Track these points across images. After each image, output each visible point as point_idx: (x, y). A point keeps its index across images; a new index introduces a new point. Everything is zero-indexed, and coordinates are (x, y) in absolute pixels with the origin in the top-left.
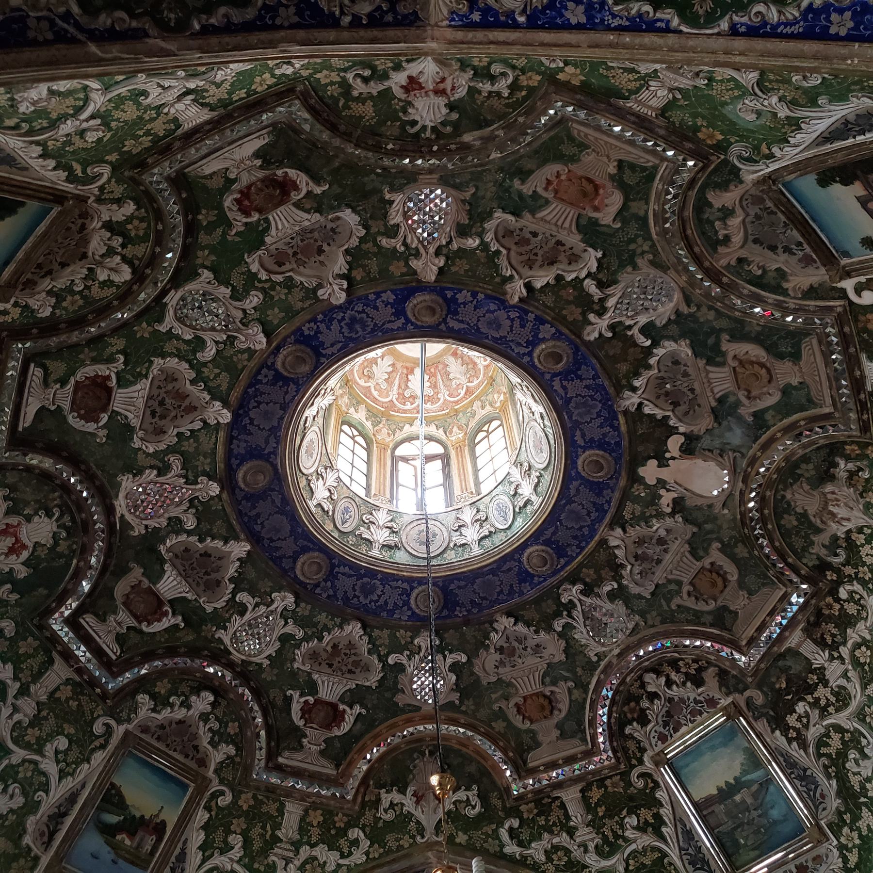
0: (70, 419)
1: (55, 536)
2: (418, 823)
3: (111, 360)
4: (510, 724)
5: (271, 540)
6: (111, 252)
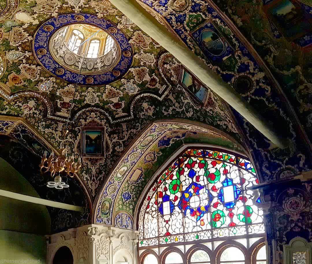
0: (123, 107)
1: (145, 102)
3: (109, 106)
5: (127, 64)
6: (90, 117)
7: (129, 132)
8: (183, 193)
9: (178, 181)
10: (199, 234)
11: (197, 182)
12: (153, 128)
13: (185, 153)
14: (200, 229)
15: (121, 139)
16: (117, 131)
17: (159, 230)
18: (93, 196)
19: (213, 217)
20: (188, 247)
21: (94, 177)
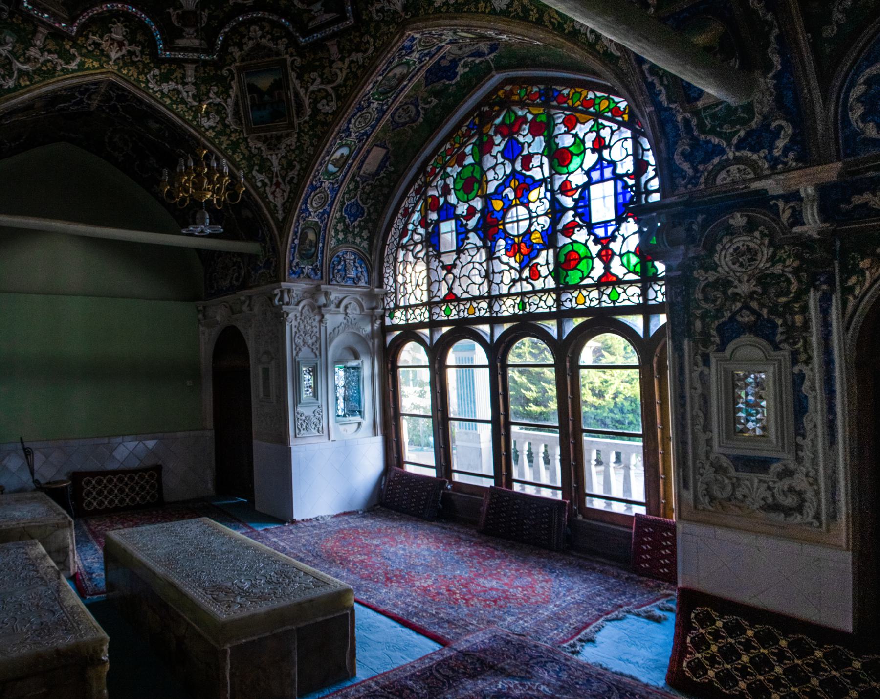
7: (347, 61)
8: (488, 199)
9: (477, 168)
11: (523, 172)
12: (407, 44)
13: (498, 96)
15: (329, 82)
16: (318, 63)
17: (432, 288)
18: (280, 218)
19: (562, 259)
21: (277, 176)
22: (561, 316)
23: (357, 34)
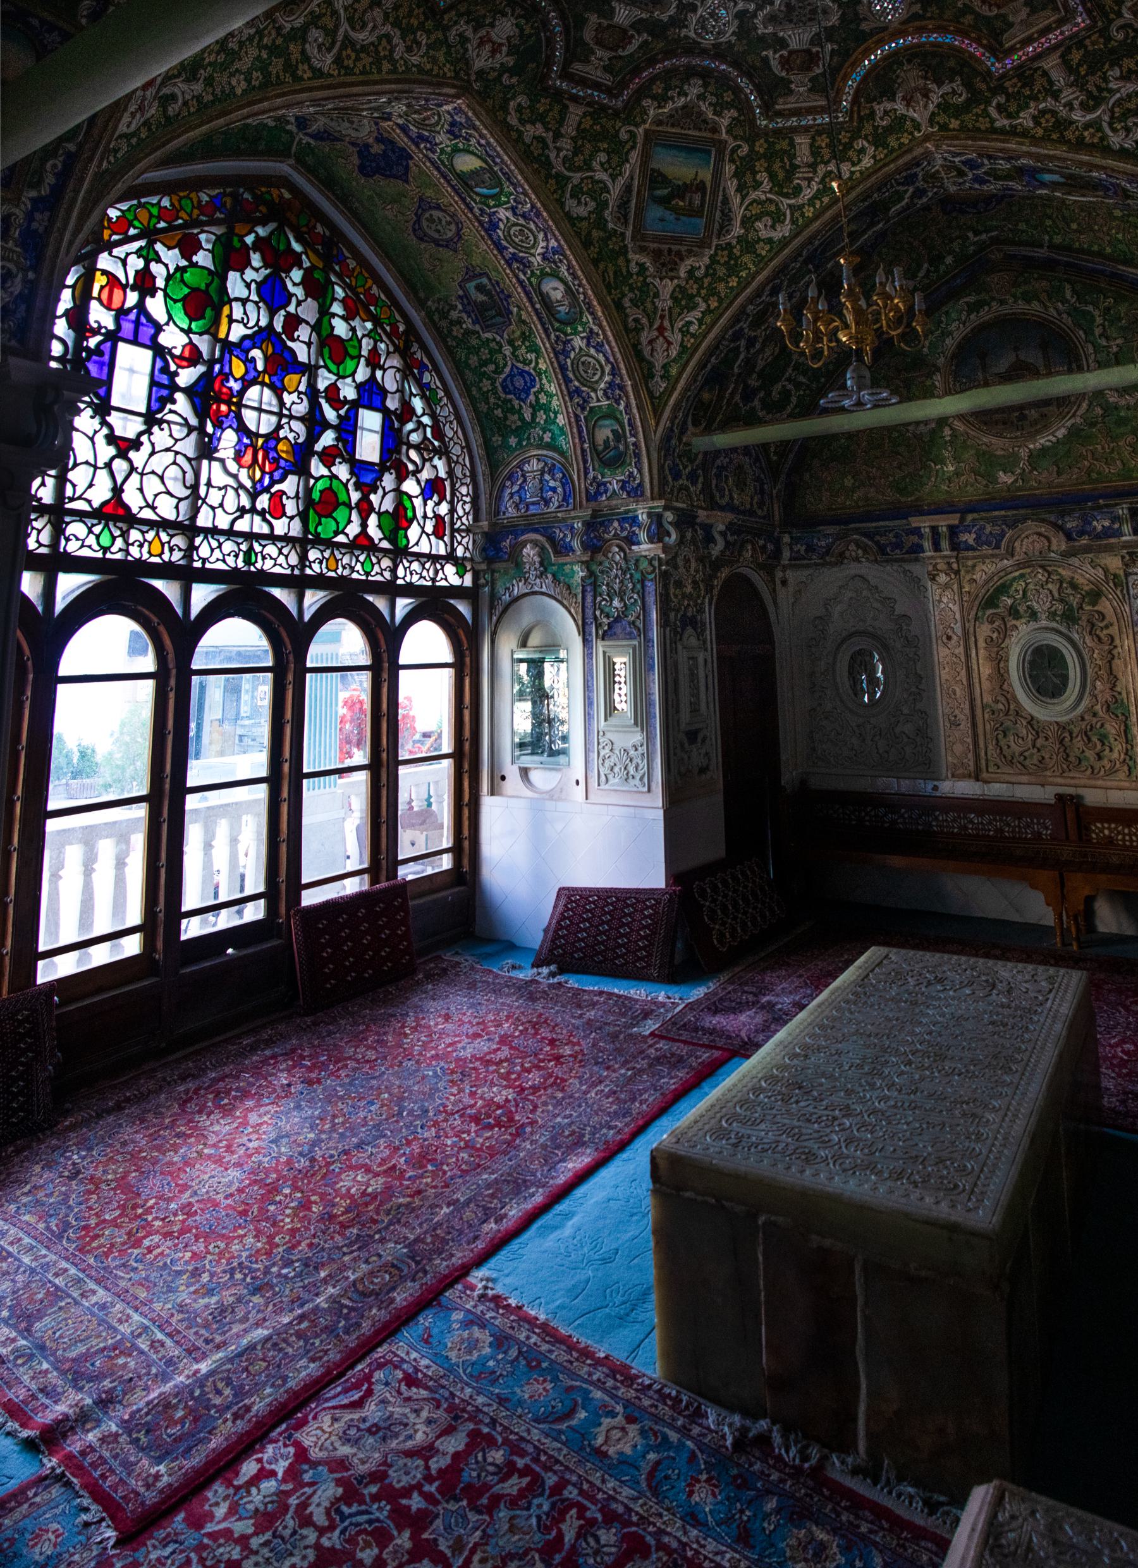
2: (913, 120)
4: (978, 16)
10: (257, 547)
14: (266, 530)
20: (70, 585)
22: (298, 583)
23: (422, 18)
